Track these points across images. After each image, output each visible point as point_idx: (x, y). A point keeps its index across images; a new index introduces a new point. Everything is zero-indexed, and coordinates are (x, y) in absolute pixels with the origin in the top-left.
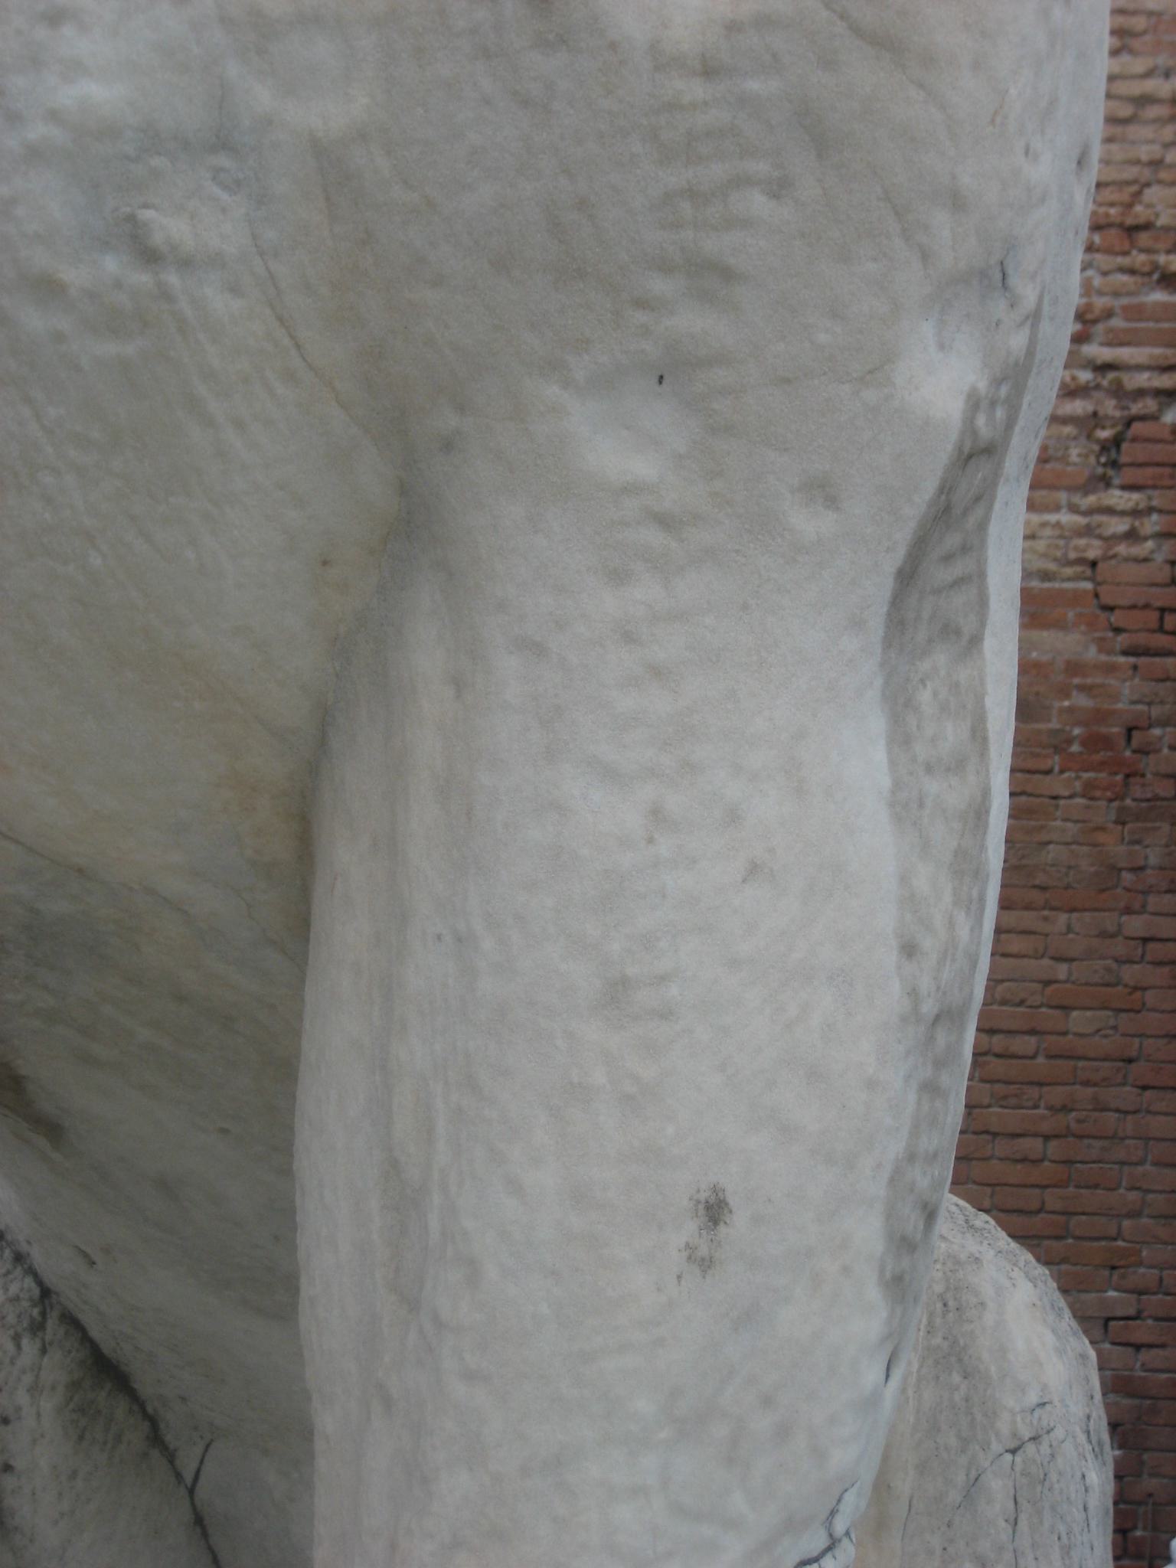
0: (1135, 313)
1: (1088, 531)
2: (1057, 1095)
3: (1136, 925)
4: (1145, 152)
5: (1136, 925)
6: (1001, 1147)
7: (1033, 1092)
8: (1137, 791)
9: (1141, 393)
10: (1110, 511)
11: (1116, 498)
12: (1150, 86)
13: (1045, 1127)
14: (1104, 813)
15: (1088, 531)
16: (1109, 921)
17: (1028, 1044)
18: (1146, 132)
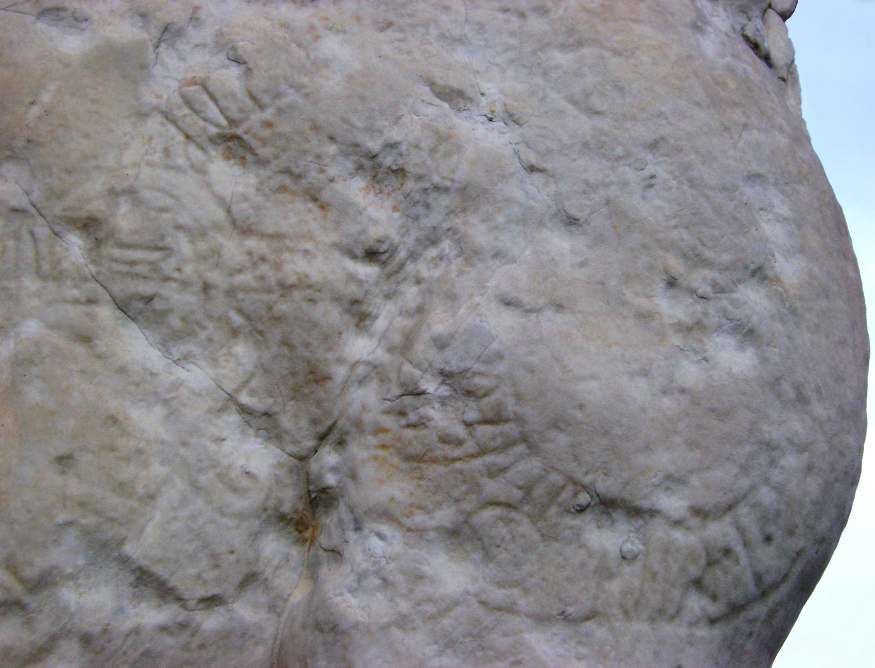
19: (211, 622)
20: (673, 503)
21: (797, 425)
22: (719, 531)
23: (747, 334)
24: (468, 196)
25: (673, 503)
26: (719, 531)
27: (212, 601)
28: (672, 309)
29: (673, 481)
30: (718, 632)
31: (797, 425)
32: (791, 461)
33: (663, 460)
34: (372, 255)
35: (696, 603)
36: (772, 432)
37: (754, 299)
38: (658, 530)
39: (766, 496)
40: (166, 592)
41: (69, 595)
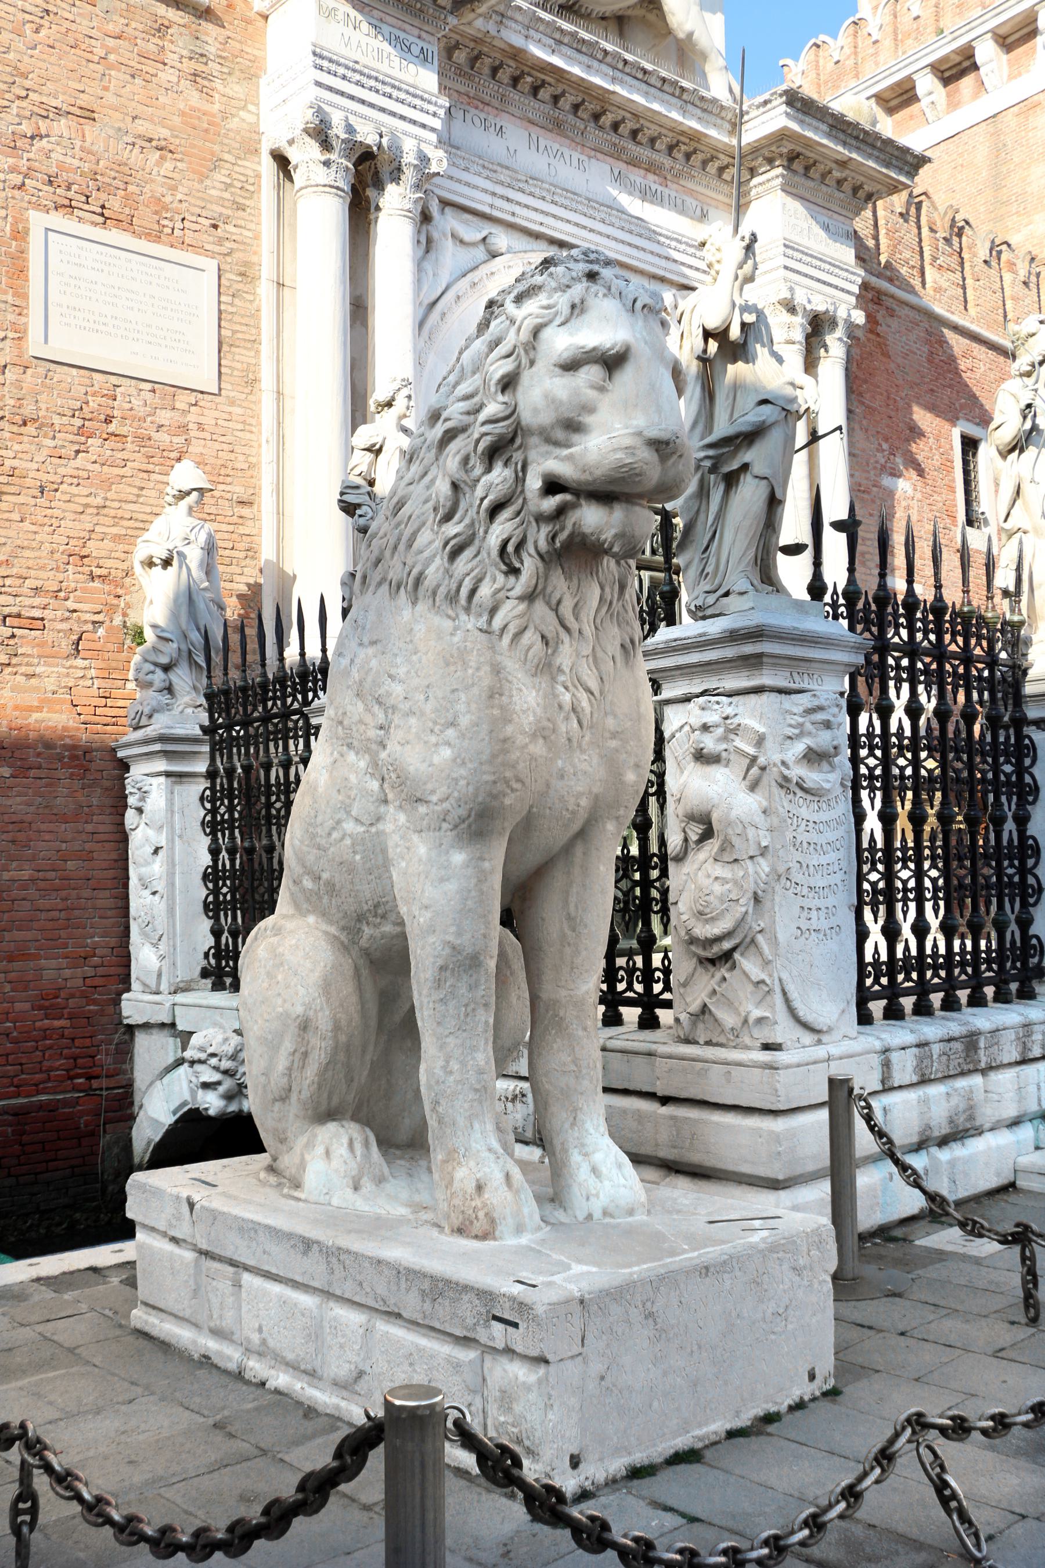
0: (85, 590)
1: (68, 675)
2: (64, 893)
3: (89, 828)
4: (89, 526)
5: (89, 828)
6: (43, 915)
7: (54, 894)
8: (88, 776)
9: (86, 622)
10: (76, 667)
11: (79, 662)
12: (89, 500)
13: (60, 907)
14: (77, 784)
15: (68, 675)
16: (80, 826)
17: (52, 875)
18: (88, 518)
19: (373, 830)
20: (434, 798)
21: (463, 772)
22: (446, 805)
23: (448, 744)
24: (394, 708)
25: (434, 798)
26: (446, 805)
27: (372, 824)
28: (433, 739)
29: (433, 792)
30: (454, 833)
31: (463, 772)
32: (463, 783)
33: (429, 786)
34: (381, 728)
35: (445, 826)
36: (455, 775)
37: (451, 733)
38: (431, 806)
39: (456, 794)
40: (362, 824)
41: (345, 825)
